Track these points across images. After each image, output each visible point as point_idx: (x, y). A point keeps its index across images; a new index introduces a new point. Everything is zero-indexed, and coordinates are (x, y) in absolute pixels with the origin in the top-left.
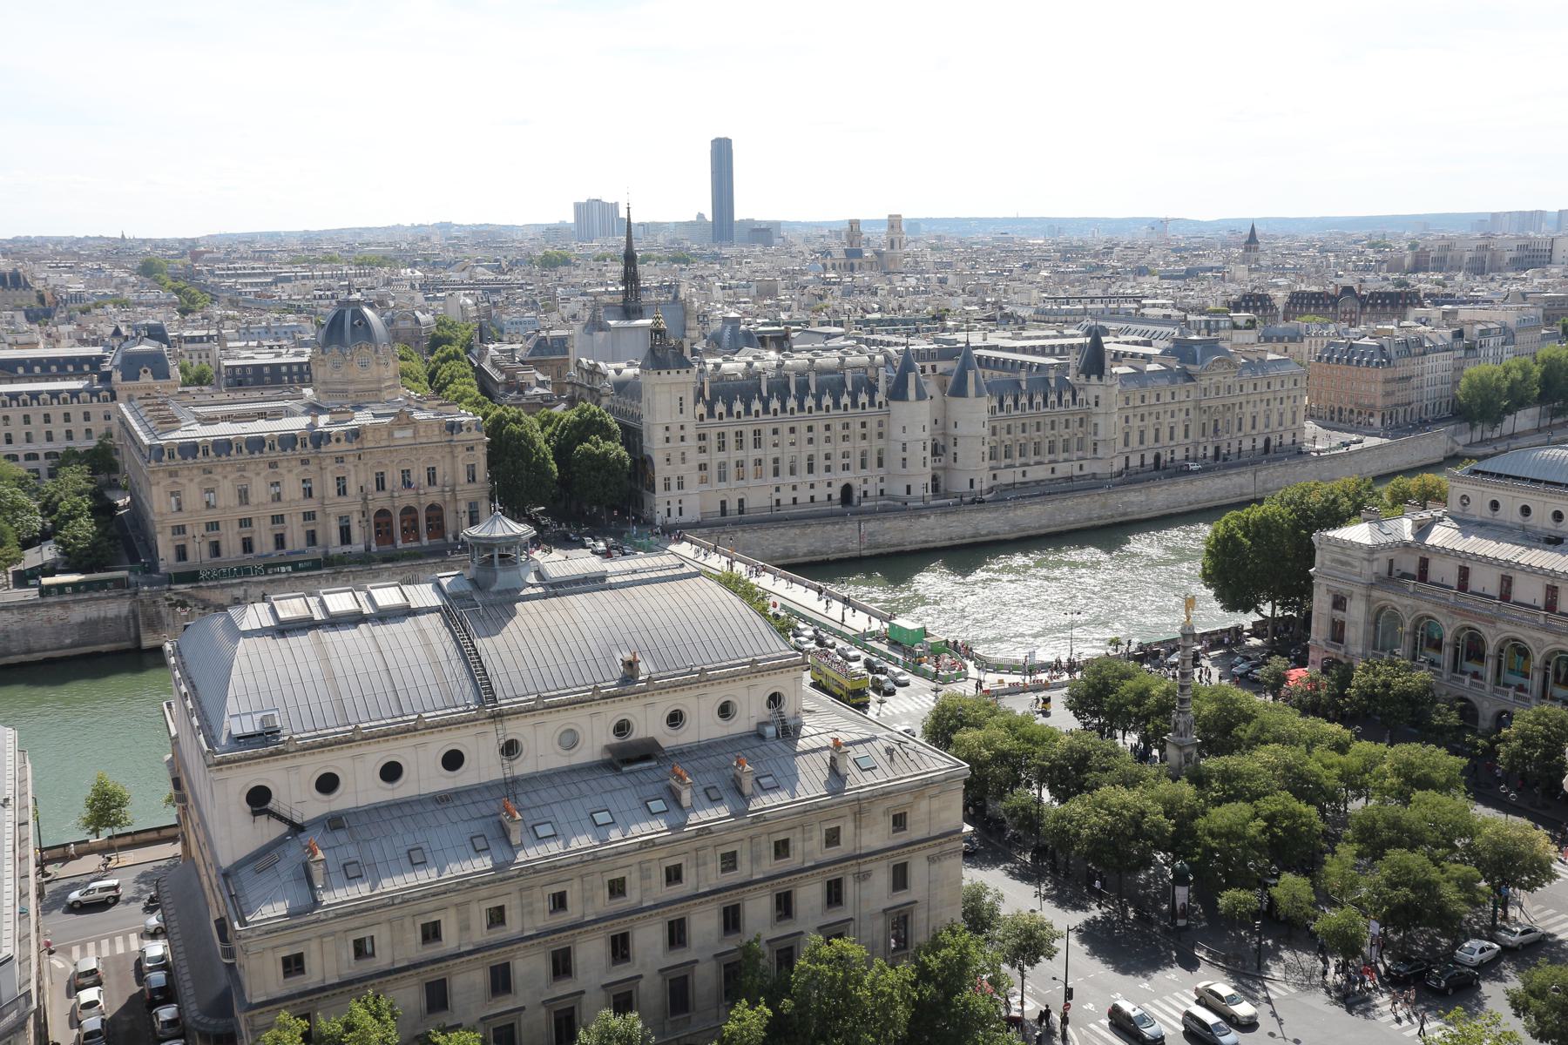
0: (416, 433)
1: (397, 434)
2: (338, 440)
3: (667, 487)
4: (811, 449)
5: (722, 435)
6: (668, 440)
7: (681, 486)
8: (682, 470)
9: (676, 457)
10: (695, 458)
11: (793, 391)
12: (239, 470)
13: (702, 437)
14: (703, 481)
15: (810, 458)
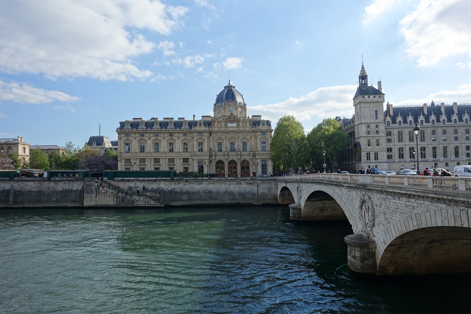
0: (238, 125)
1: (229, 125)
2: (200, 125)
3: (368, 158)
4: (457, 143)
5: (400, 134)
6: (369, 133)
7: (376, 158)
8: (377, 149)
9: (373, 142)
10: (384, 144)
11: (444, 113)
12: (156, 136)
13: (389, 134)
14: (389, 157)
15: (456, 149)
